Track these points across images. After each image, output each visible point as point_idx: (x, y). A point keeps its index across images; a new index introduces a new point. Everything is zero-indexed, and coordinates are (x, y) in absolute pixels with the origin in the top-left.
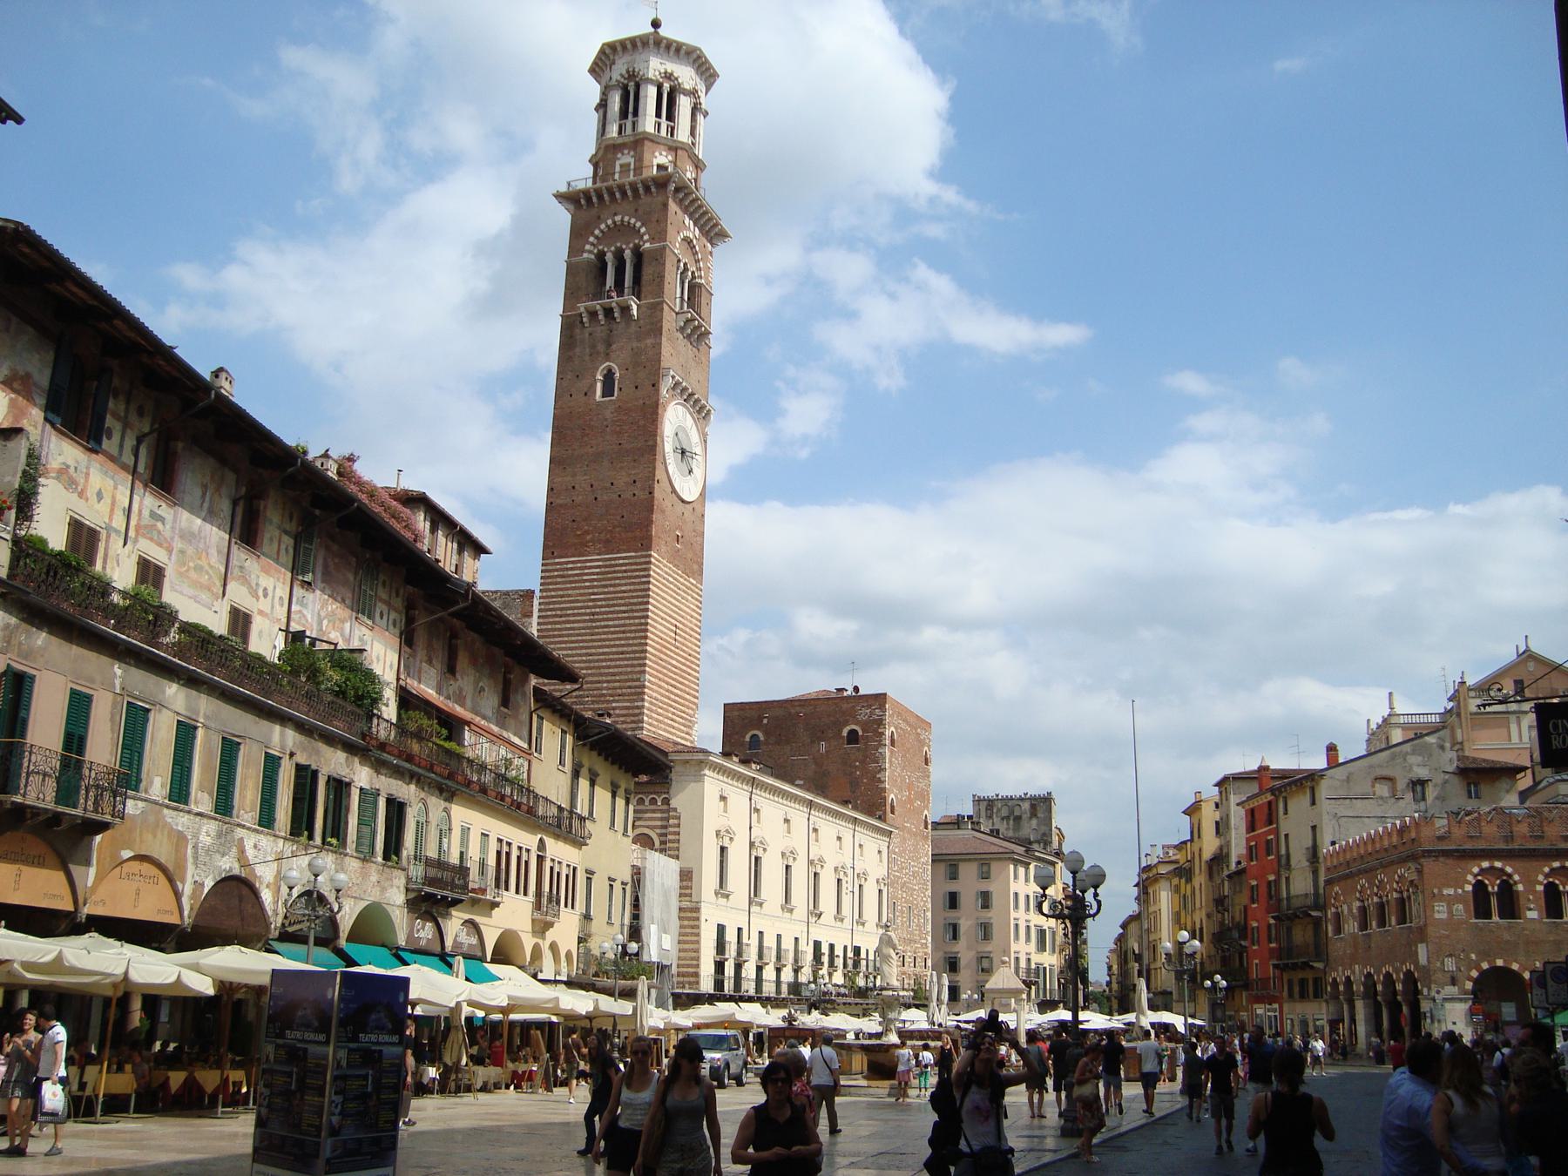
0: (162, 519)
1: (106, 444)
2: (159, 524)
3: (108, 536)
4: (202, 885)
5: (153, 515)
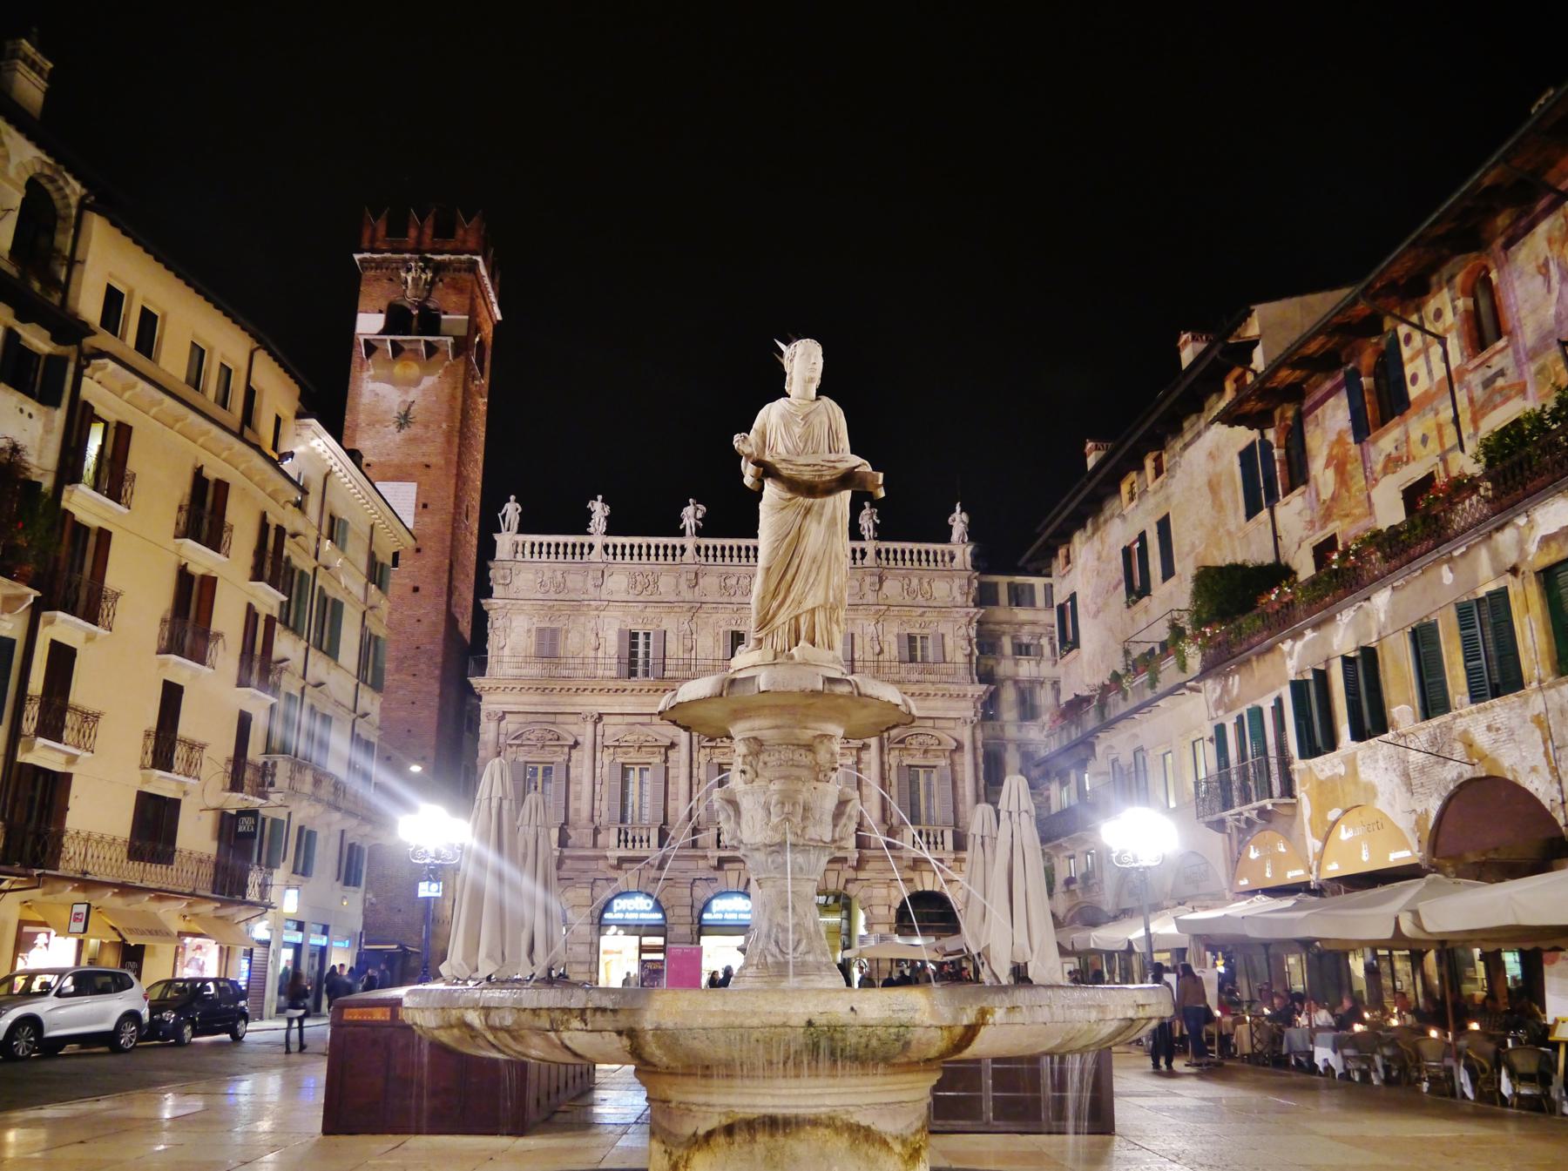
0: (1501, 373)
2: (1500, 382)
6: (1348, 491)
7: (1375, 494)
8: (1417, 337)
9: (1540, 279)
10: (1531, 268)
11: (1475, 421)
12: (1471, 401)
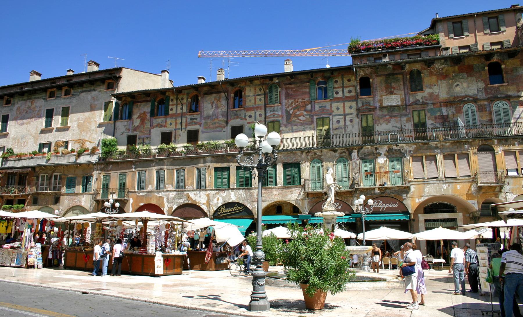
0: (196, 119)
1: (170, 112)
2: (195, 120)
3: (176, 132)
4: (172, 207)
5: (191, 119)
6: (144, 126)
7: (152, 130)
8: (175, 102)
9: (210, 105)
10: (209, 102)
11: (186, 125)
12: (186, 121)
